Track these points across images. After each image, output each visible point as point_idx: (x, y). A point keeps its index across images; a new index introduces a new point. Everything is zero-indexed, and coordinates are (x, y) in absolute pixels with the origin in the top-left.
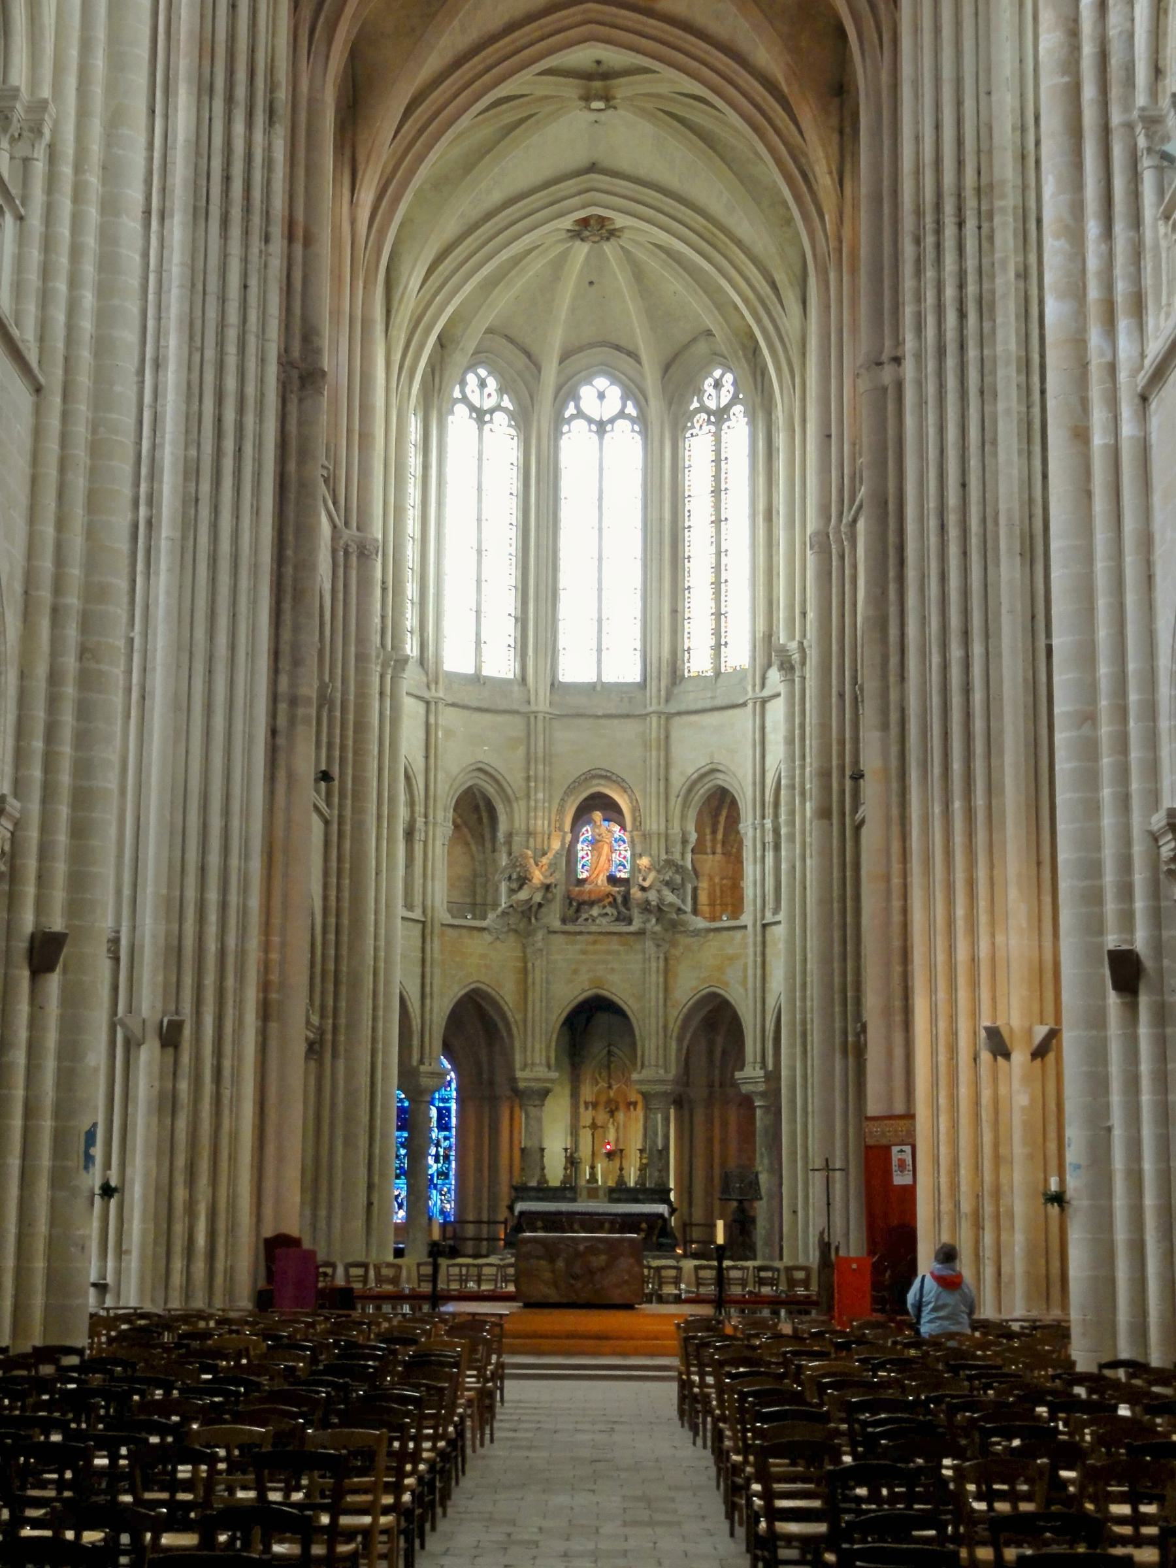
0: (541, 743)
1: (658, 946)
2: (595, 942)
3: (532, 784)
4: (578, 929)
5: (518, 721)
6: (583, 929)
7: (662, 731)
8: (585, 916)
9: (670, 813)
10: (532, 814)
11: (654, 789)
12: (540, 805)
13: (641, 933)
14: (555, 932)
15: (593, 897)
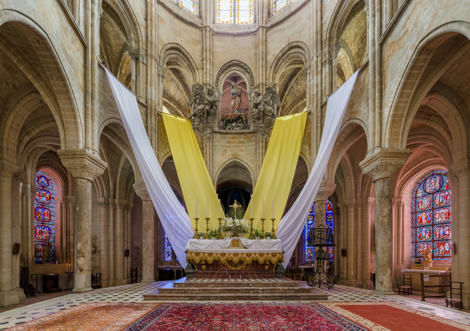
0: (208, 42)
1: (263, 135)
2: (234, 138)
3: (204, 62)
4: (226, 131)
5: (197, 32)
6: (229, 132)
7: (264, 37)
8: (230, 127)
9: (268, 76)
10: (205, 76)
11: (261, 63)
12: (208, 71)
13: (254, 132)
14: (216, 132)
15: (233, 118)
